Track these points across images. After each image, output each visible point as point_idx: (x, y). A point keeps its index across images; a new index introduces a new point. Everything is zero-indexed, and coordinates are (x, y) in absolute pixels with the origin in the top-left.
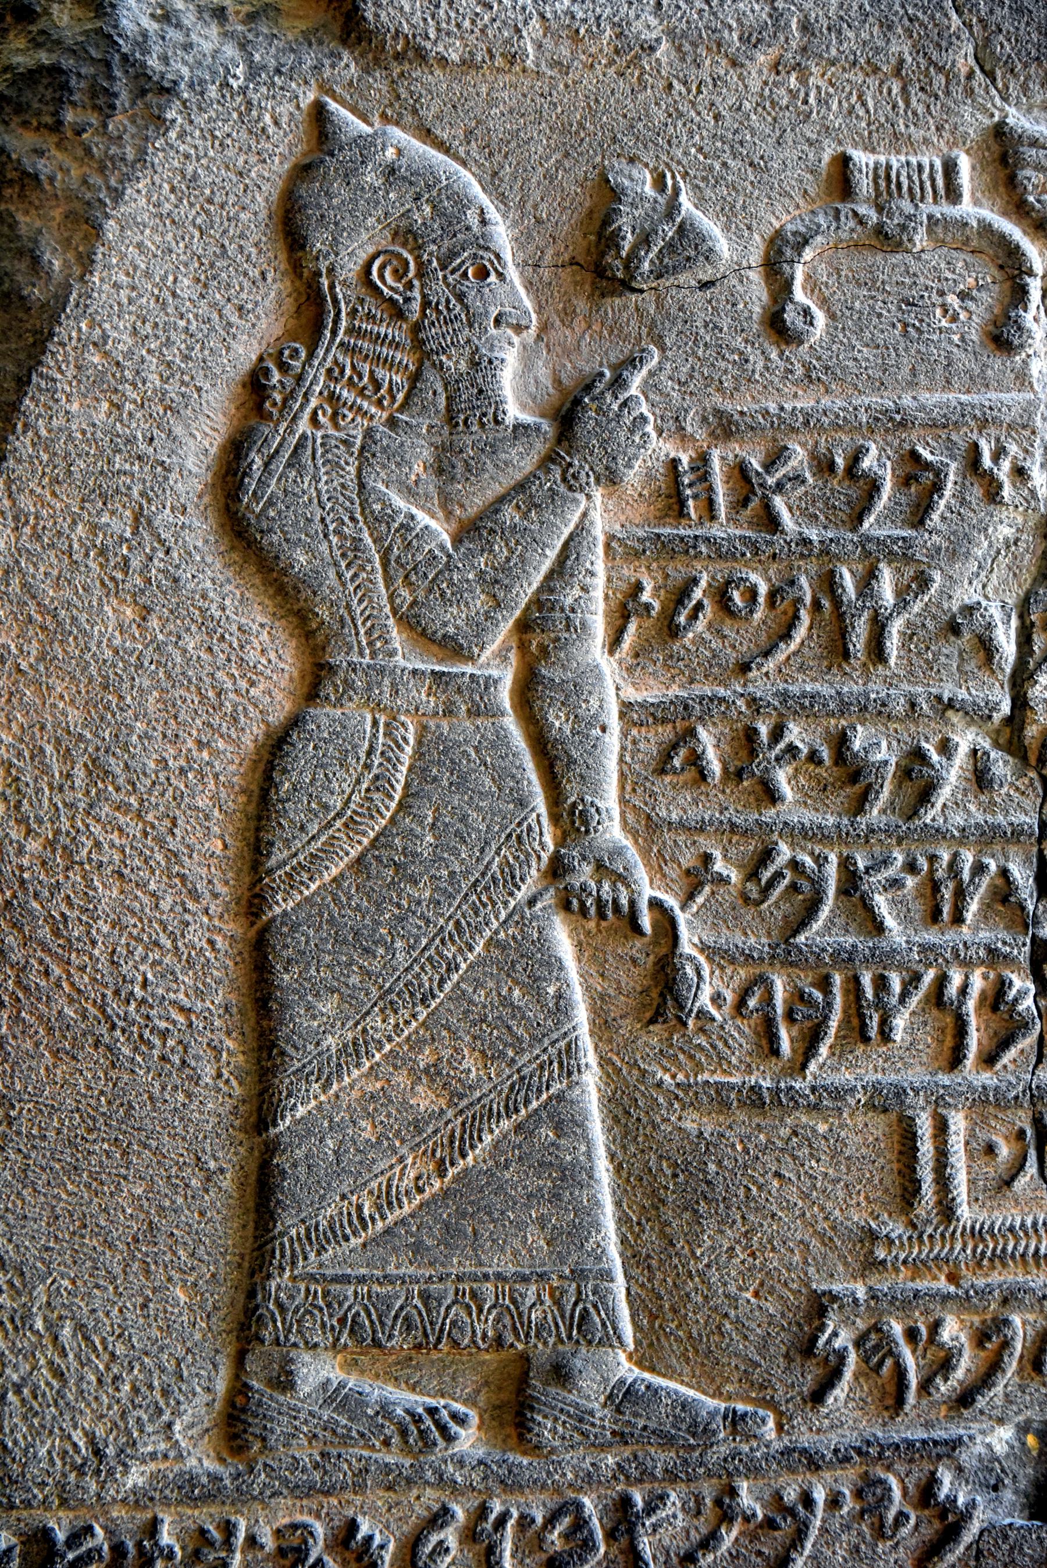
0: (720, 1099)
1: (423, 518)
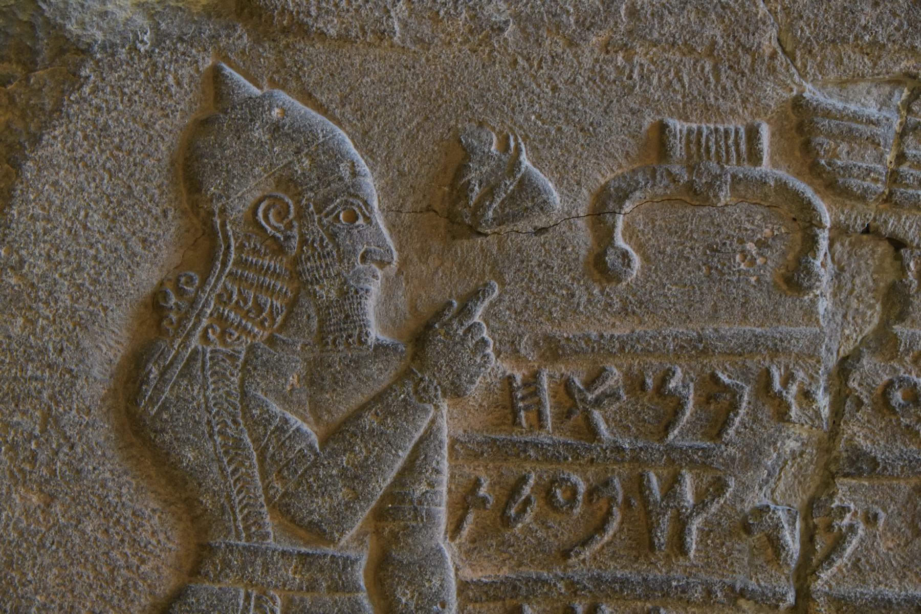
1: (295, 421)
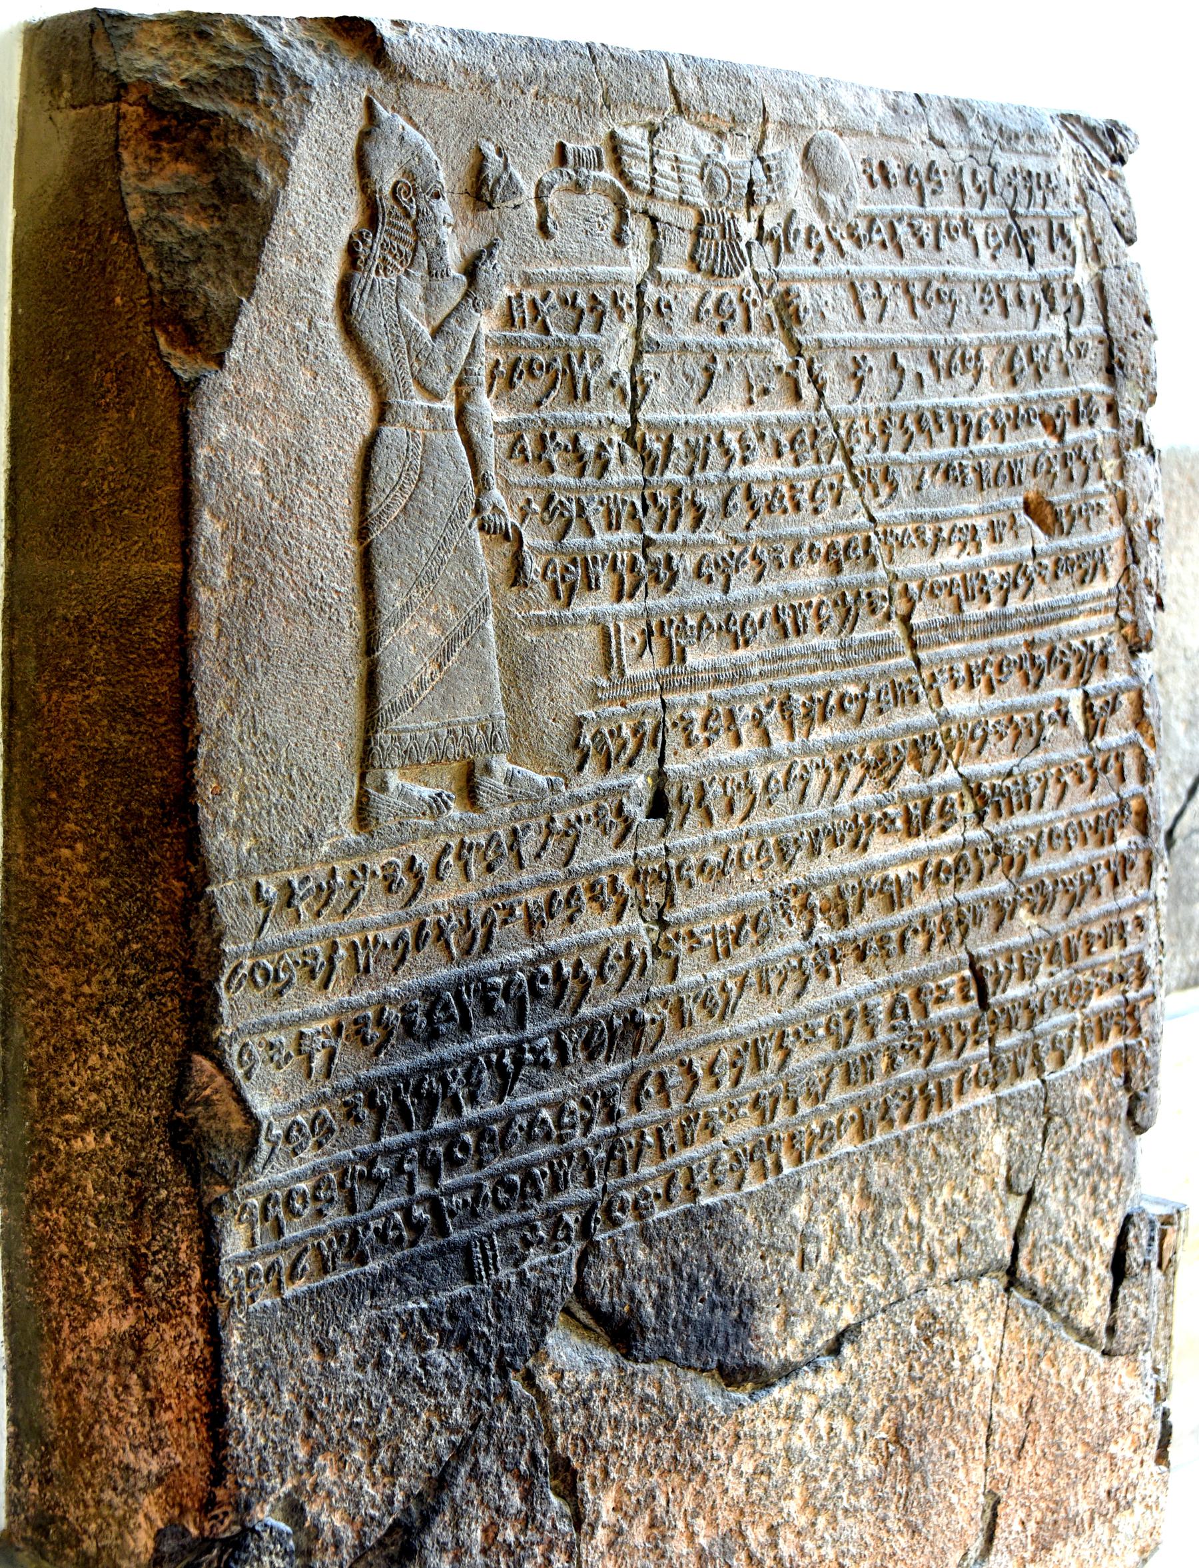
0: (539, 623)
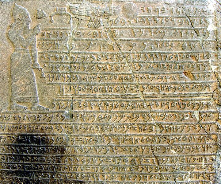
0: (45, 84)
